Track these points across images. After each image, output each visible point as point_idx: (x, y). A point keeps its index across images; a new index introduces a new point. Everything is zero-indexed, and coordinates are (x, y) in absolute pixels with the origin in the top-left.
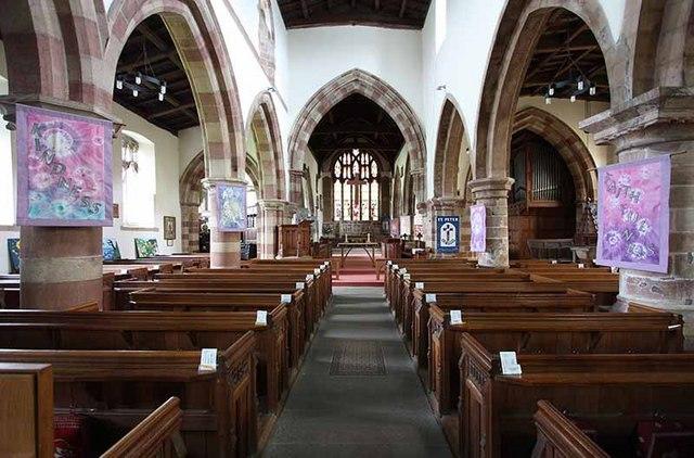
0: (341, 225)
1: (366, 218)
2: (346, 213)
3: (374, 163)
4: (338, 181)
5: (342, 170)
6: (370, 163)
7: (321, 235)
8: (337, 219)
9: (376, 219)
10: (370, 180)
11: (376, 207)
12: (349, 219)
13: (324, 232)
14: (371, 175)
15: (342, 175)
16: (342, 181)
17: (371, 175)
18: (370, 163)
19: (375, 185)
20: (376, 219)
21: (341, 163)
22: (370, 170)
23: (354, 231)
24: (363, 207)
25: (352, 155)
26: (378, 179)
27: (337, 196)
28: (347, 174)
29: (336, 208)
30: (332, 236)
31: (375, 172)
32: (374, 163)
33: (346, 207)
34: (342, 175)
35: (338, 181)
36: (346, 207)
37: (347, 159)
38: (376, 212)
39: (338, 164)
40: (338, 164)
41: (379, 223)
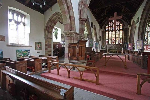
0: (108, 47)
1: (117, 43)
2: (110, 42)
3: (121, 24)
4: (107, 32)
5: (109, 28)
6: (119, 24)
7: (100, 49)
8: (106, 44)
9: (121, 44)
10: (119, 30)
11: (122, 39)
12: (111, 44)
13: (102, 48)
14: (119, 28)
15: (108, 30)
16: (109, 31)
17: (119, 28)
18: (119, 24)
19: (121, 32)
20: (121, 44)
21: (108, 26)
22: (112, 28)
23: (113, 48)
24: (116, 40)
25: (112, 22)
26: (123, 30)
27: (107, 36)
28: (110, 29)
29: (106, 40)
30: (104, 50)
31: (121, 27)
32: (121, 24)
33: (110, 40)
34: (108, 30)
35: (107, 32)
36: (110, 40)
37: (110, 24)
38: (121, 41)
39: (107, 26)
40: (107, 26)
41: (123, 45)
